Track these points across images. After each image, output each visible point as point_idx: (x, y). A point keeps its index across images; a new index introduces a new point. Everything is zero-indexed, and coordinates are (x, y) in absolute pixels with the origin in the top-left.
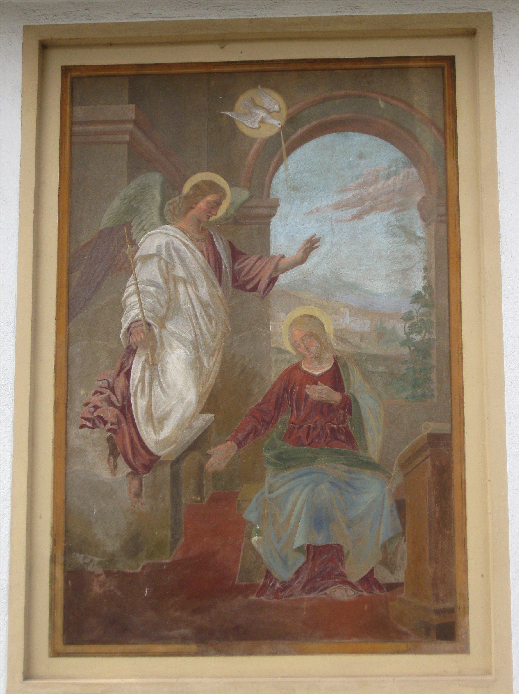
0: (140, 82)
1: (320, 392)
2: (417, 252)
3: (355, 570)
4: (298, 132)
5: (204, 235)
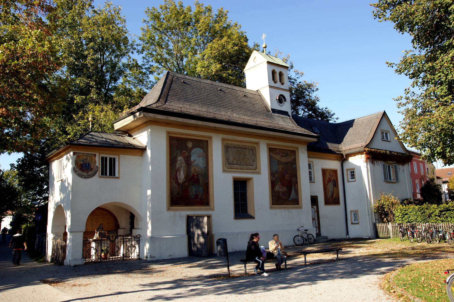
0: (178, 139)
1: (196, 177)
2: (205, 162)
3: (199, 197)
4: (194, 147)
5: (184, 158)
